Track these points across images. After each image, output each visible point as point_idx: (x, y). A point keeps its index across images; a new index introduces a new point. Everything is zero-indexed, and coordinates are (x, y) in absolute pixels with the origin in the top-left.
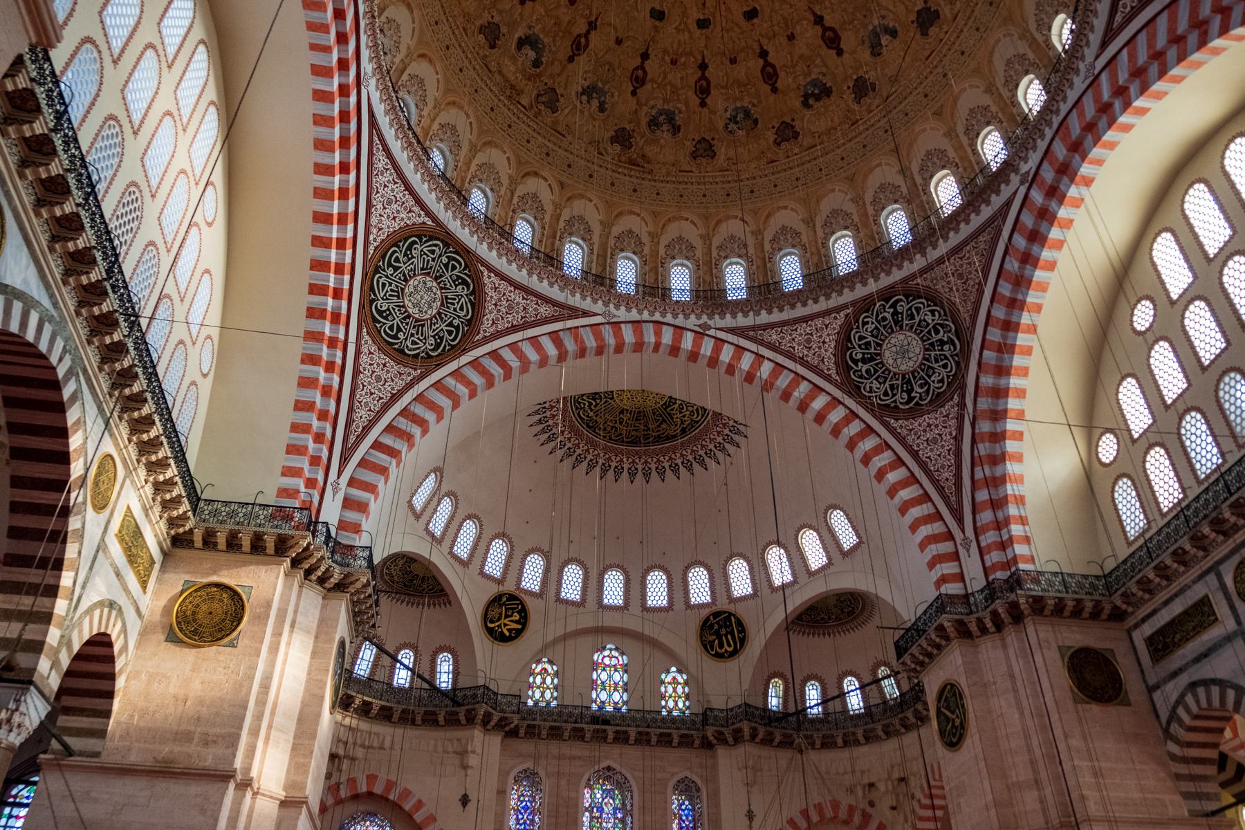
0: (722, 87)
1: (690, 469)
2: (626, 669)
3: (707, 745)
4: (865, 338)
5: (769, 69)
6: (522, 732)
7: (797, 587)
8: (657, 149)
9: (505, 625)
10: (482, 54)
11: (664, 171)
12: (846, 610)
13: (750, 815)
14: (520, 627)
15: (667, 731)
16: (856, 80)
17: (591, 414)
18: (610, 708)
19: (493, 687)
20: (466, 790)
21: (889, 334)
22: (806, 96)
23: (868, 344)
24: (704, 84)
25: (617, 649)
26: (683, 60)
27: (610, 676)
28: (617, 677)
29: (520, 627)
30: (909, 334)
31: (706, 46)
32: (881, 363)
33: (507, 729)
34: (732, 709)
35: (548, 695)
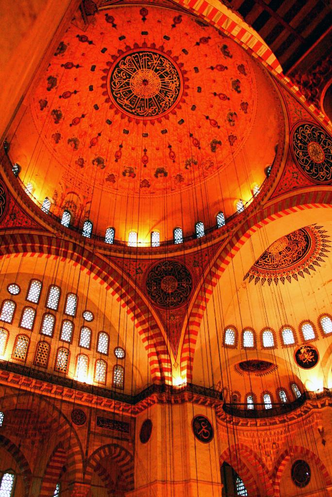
0: (218, 116)
1: (326, 251)
4: (304, 159)
5: (221, 96)
8: (221, 156)
10: (147, 192)
11: (228, 160)
16: (238, 69)
17: (270, 263)
21: (307, 150)
22: (236, 90)
23: (306, 161)
24: (212, 122)
26: (201, 123)
30: (311, 144)
31: (202, 112)
32: (316, 163)
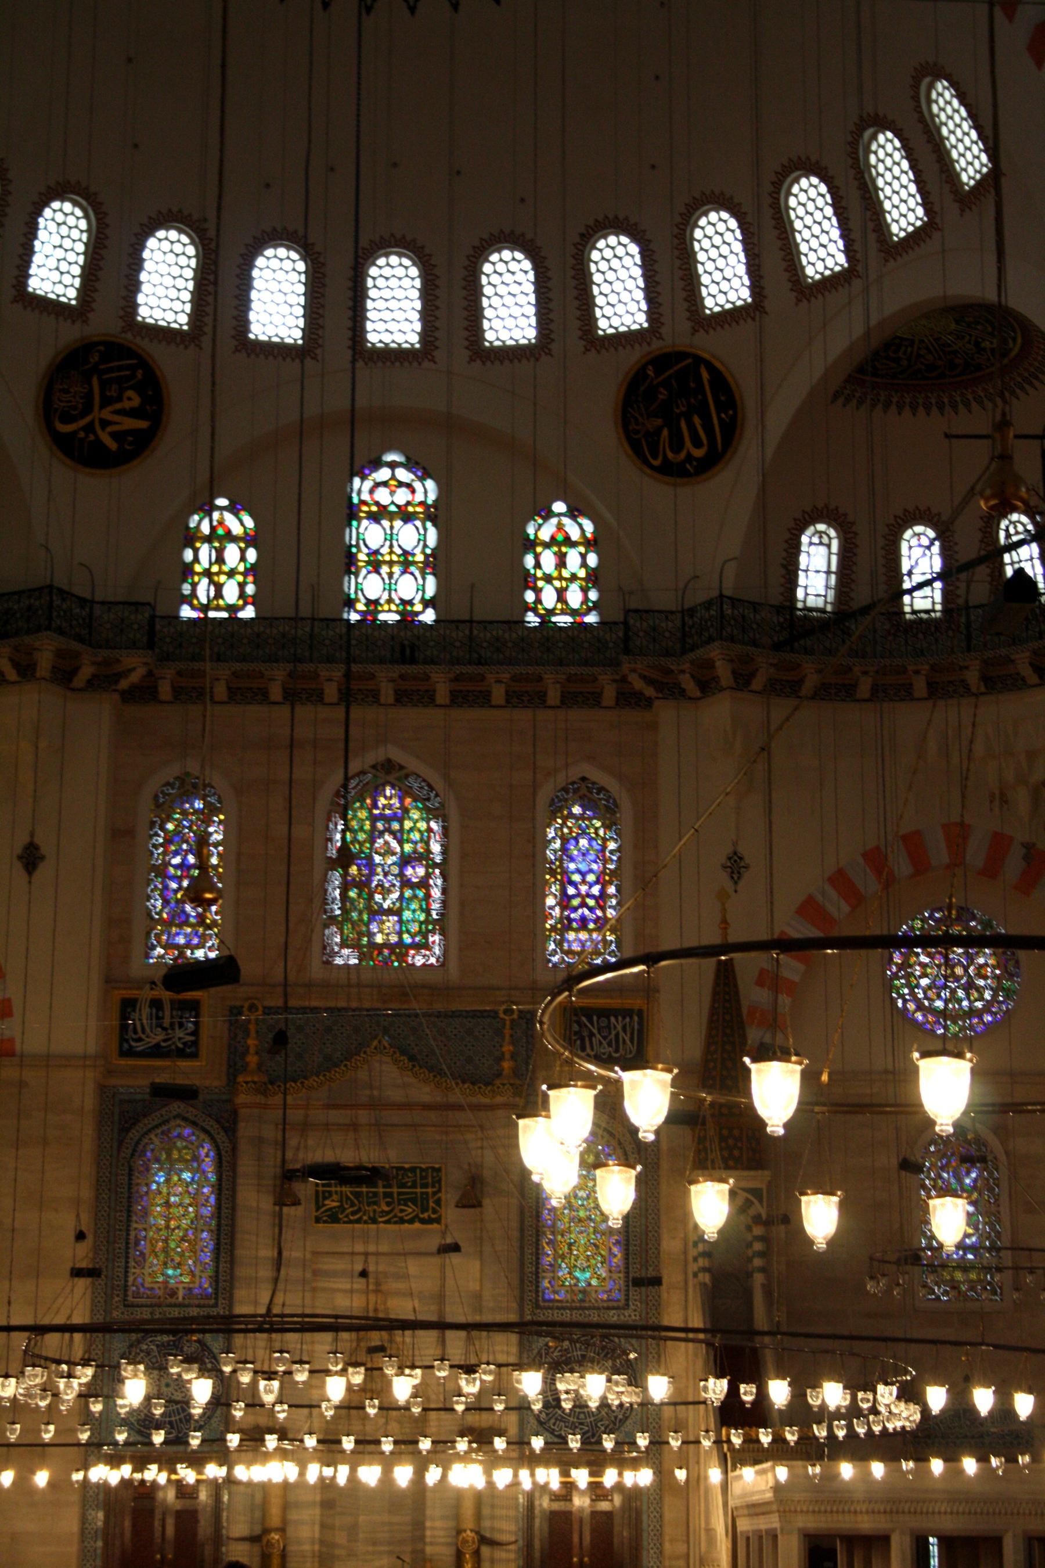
2: (433, 514)
3: (629, 699)
6: (165, 689)
7: (857, 284)
9: (104, 424)
12: (986, 344)
13: (735, 866)
14: (143, 424)
15: (530, 670)
18: (389, 617)
19: (81, 590)
20: (32, 835)
25: (410, 465)
27: (390, 537)
28: (408, 536)
29: (143, 424)
33: (124, 684)
34: (692, 611)
35: (231, 593)
